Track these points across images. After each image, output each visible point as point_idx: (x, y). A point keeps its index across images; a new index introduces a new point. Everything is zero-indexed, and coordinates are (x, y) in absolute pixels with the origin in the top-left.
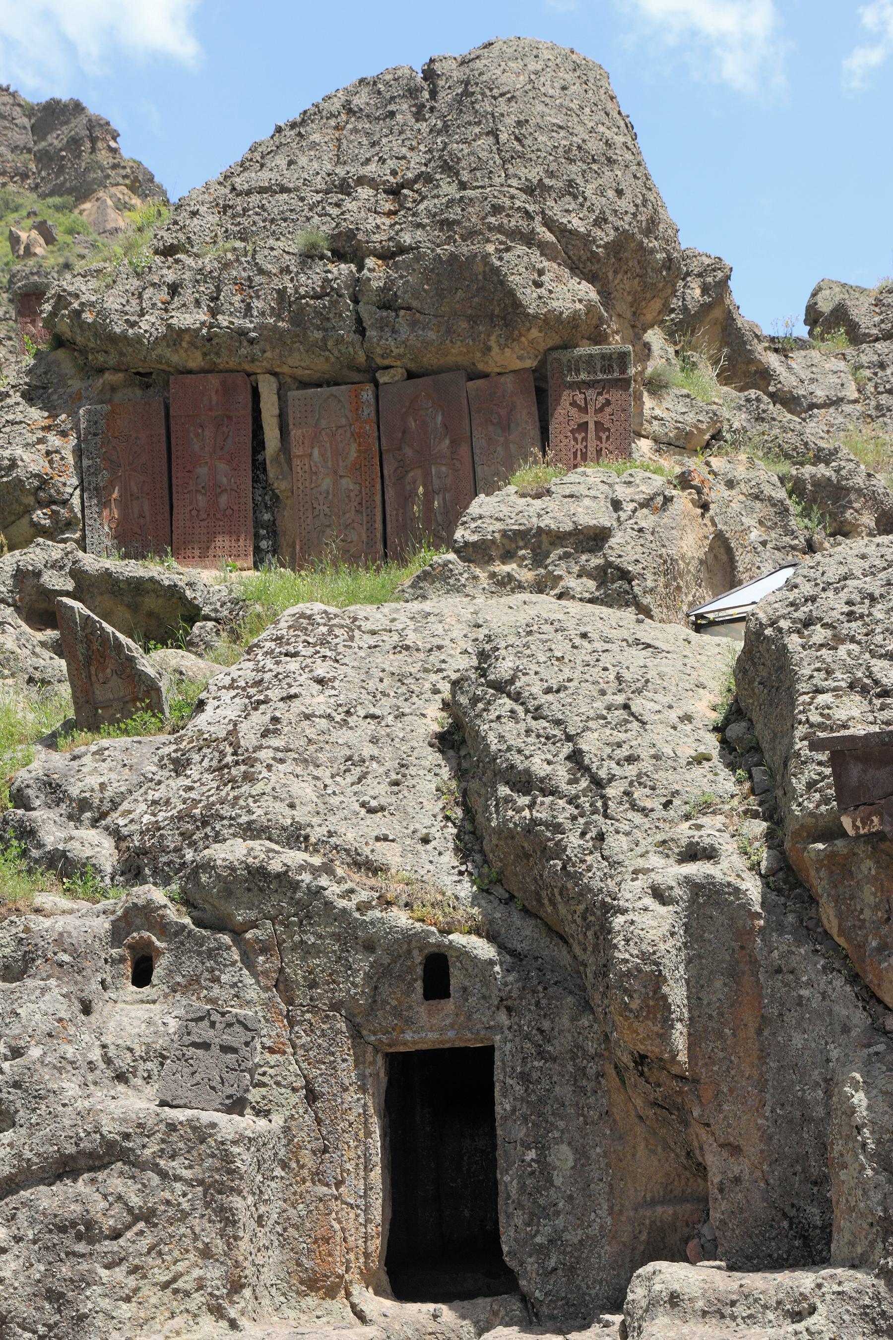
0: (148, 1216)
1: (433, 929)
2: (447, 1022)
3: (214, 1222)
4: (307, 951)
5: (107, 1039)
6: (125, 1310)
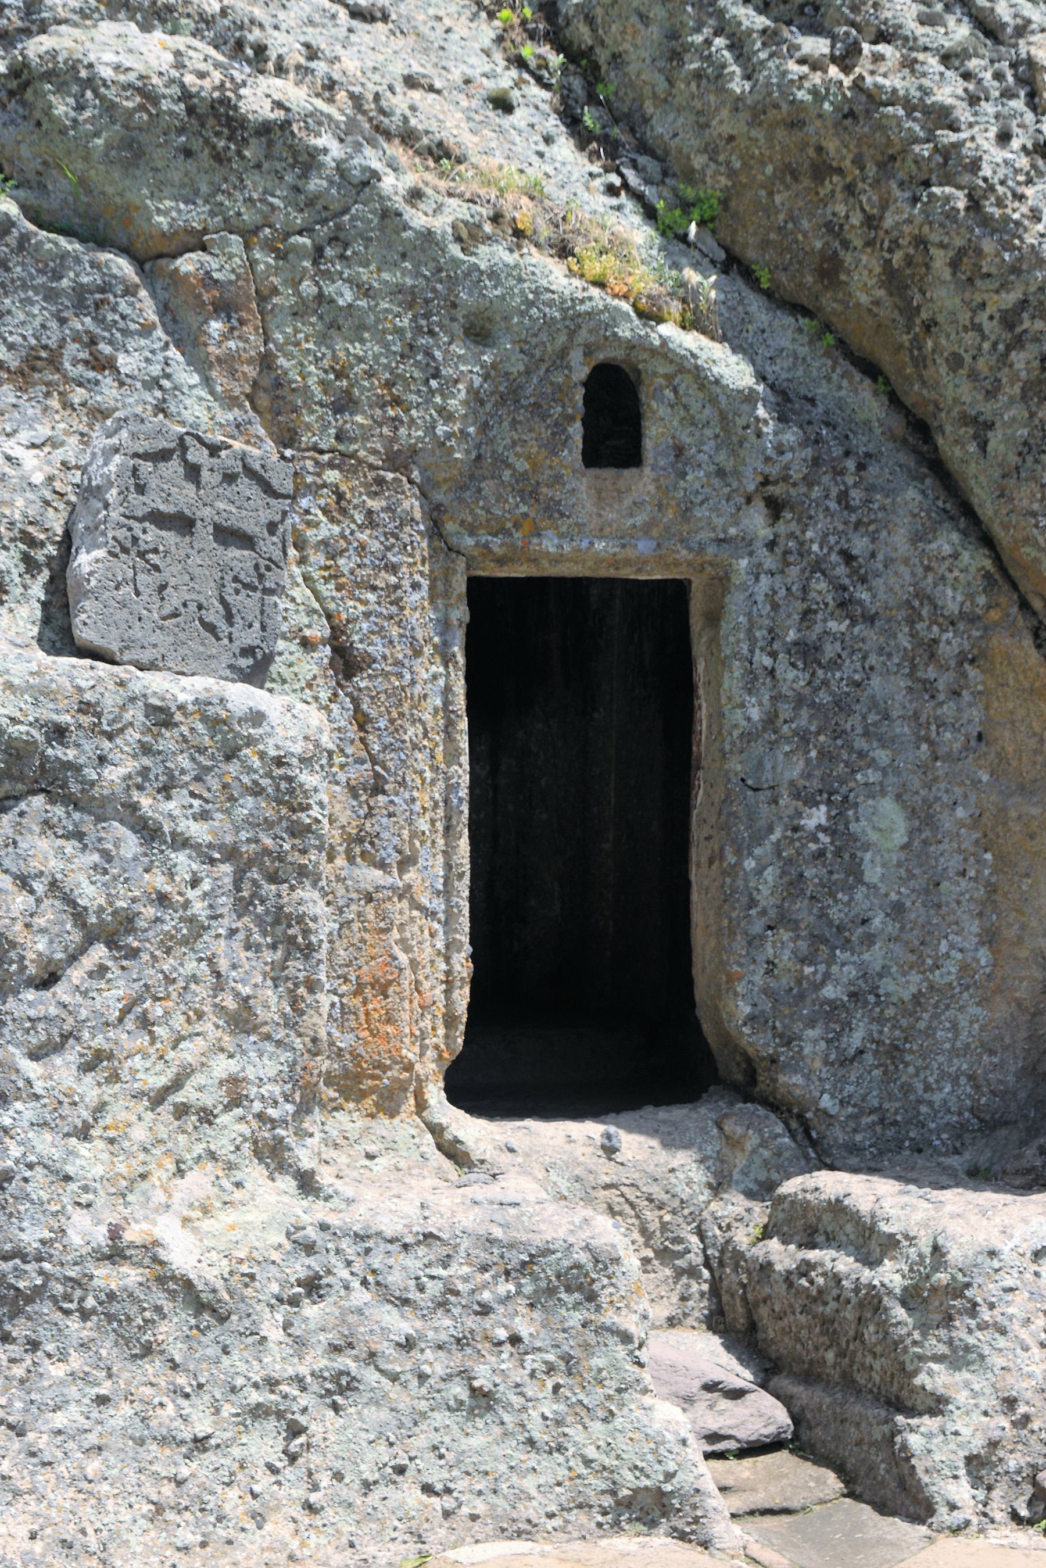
0: (115, 932)
1: (625, 306)
2: (640, 519)
3: (258, 948)
4: (334, 321)
6: (90, 1160)
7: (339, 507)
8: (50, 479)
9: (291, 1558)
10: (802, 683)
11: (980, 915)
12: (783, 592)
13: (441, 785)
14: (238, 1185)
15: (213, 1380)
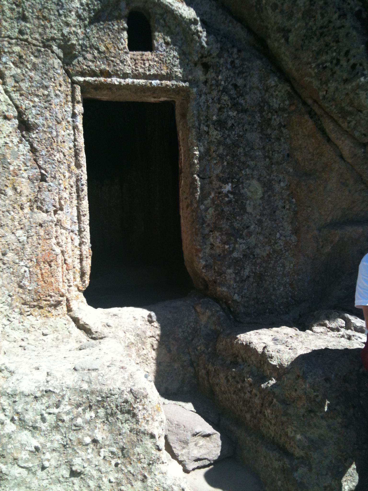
10: (220, 136)
11: (291, 223)
12: (210, 101)
13: (74, 179)
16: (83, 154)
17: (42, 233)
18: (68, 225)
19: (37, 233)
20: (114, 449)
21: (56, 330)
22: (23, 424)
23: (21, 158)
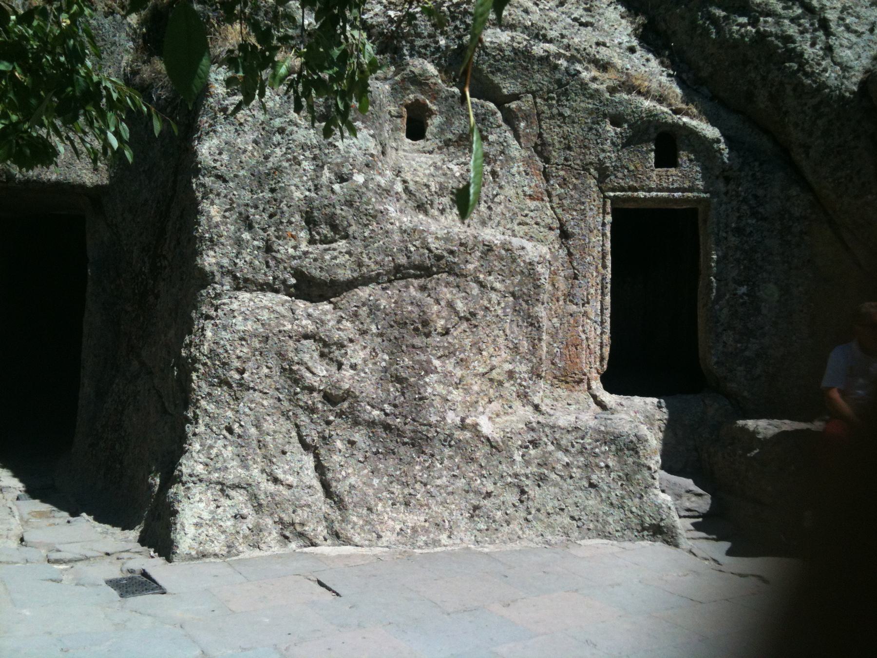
5: (408, 177)
6: (456, 395)
7: (564, 183)
8: (461, 175)
9: (519, 537)
14: (510, 407)
15: (496, 473)
16: (609, 257)
17: (572, 321)
18: (592, 317)
19: (568, 322)
20: (621, 474)
21: (578, 403)
22: (559, 447)
23: (560, 260)
